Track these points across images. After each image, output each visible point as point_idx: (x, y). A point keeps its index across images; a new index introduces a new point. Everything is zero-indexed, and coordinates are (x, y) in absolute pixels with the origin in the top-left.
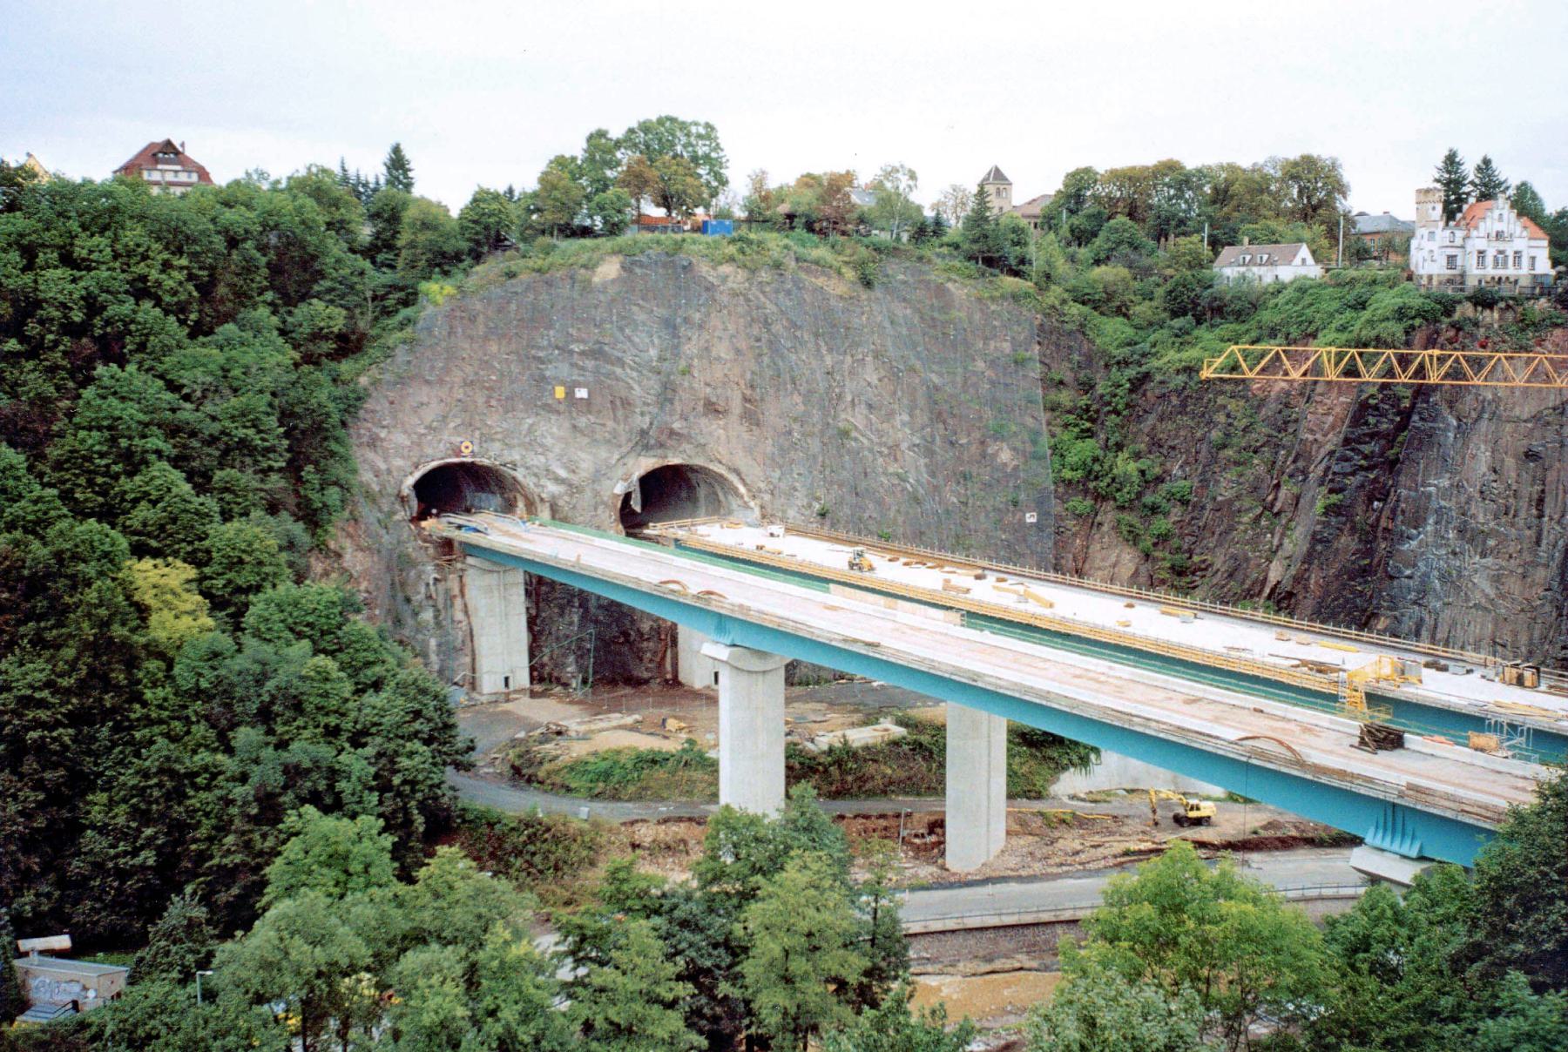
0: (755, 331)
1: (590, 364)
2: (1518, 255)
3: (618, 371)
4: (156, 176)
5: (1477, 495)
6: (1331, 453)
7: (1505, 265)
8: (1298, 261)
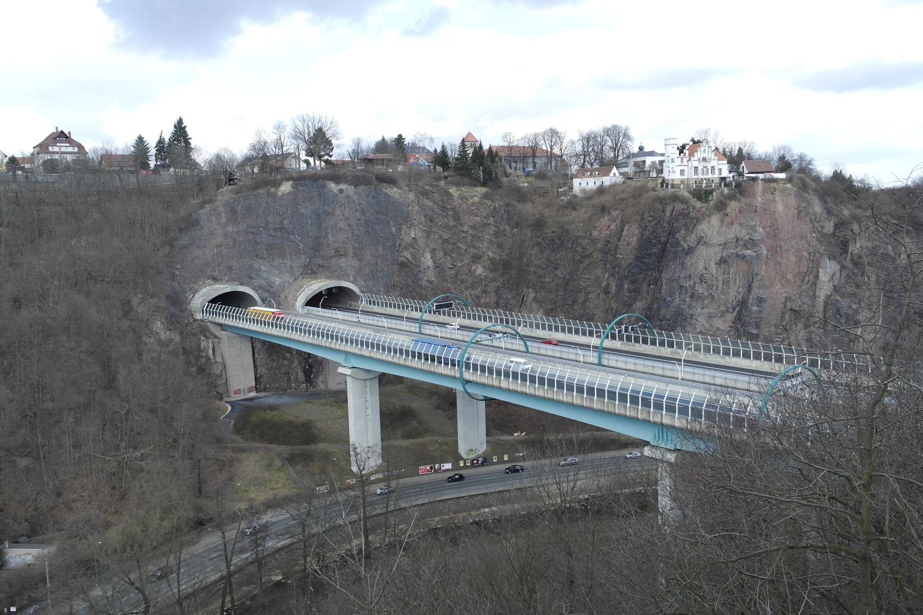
1: (279, 234)
2: (713, 168)
3: (292, 237)
4: (56, 149)
5: (698, 281)
6: (631, 264)
7: (707, 174)
8: (612, 174)
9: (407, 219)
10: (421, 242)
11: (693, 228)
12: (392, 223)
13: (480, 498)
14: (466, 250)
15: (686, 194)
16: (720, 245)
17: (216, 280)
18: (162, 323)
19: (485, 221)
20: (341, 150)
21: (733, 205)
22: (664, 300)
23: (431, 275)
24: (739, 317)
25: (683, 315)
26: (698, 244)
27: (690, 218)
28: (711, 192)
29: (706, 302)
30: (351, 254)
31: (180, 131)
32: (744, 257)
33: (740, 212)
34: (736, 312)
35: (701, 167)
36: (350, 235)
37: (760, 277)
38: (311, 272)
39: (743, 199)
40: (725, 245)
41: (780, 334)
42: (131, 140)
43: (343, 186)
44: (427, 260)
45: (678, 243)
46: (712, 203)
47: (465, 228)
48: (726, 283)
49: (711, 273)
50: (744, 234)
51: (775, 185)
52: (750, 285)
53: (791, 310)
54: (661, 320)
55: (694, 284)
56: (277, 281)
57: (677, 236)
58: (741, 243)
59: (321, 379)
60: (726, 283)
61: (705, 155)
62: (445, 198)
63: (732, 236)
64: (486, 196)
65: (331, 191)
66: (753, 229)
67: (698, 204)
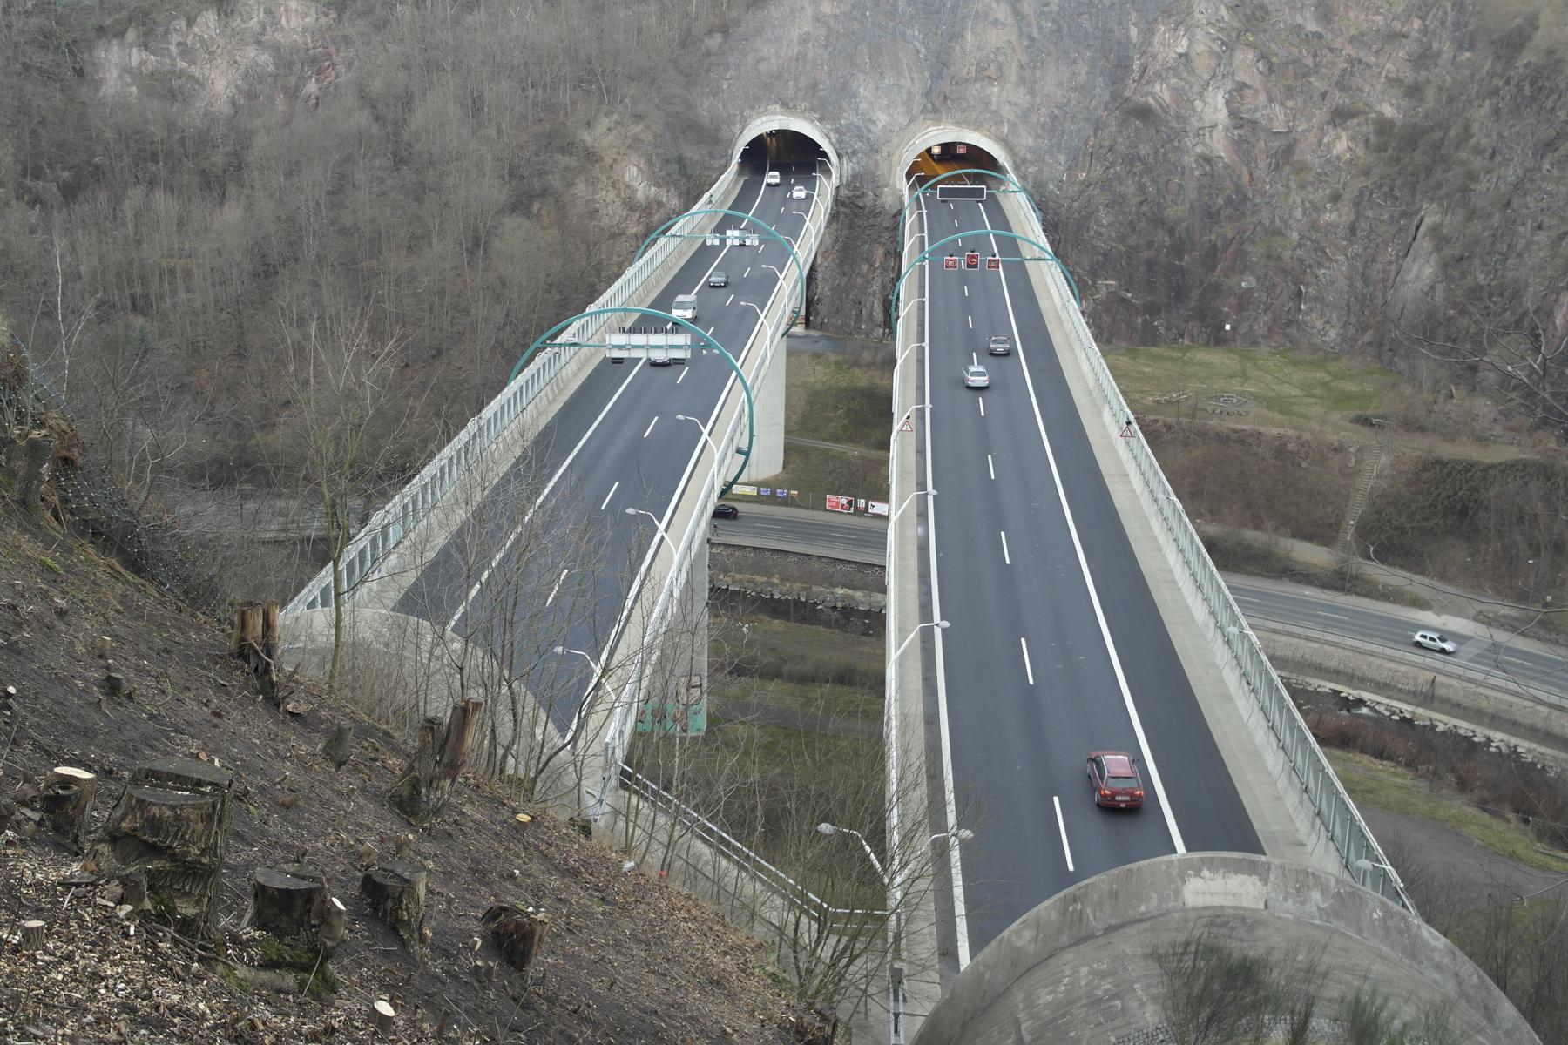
3: (909, 32)
10: (1203, 66)
12: (1134, 16)
13: (849, 568)
14: (1324, 95)
17: (787, 106)
18: (640, 169)
19: (1397, 25)
23: (1218, 144)
36: (1013, 38)
38: (937, 105)
44: (1214, 108)
56: (882, 118)
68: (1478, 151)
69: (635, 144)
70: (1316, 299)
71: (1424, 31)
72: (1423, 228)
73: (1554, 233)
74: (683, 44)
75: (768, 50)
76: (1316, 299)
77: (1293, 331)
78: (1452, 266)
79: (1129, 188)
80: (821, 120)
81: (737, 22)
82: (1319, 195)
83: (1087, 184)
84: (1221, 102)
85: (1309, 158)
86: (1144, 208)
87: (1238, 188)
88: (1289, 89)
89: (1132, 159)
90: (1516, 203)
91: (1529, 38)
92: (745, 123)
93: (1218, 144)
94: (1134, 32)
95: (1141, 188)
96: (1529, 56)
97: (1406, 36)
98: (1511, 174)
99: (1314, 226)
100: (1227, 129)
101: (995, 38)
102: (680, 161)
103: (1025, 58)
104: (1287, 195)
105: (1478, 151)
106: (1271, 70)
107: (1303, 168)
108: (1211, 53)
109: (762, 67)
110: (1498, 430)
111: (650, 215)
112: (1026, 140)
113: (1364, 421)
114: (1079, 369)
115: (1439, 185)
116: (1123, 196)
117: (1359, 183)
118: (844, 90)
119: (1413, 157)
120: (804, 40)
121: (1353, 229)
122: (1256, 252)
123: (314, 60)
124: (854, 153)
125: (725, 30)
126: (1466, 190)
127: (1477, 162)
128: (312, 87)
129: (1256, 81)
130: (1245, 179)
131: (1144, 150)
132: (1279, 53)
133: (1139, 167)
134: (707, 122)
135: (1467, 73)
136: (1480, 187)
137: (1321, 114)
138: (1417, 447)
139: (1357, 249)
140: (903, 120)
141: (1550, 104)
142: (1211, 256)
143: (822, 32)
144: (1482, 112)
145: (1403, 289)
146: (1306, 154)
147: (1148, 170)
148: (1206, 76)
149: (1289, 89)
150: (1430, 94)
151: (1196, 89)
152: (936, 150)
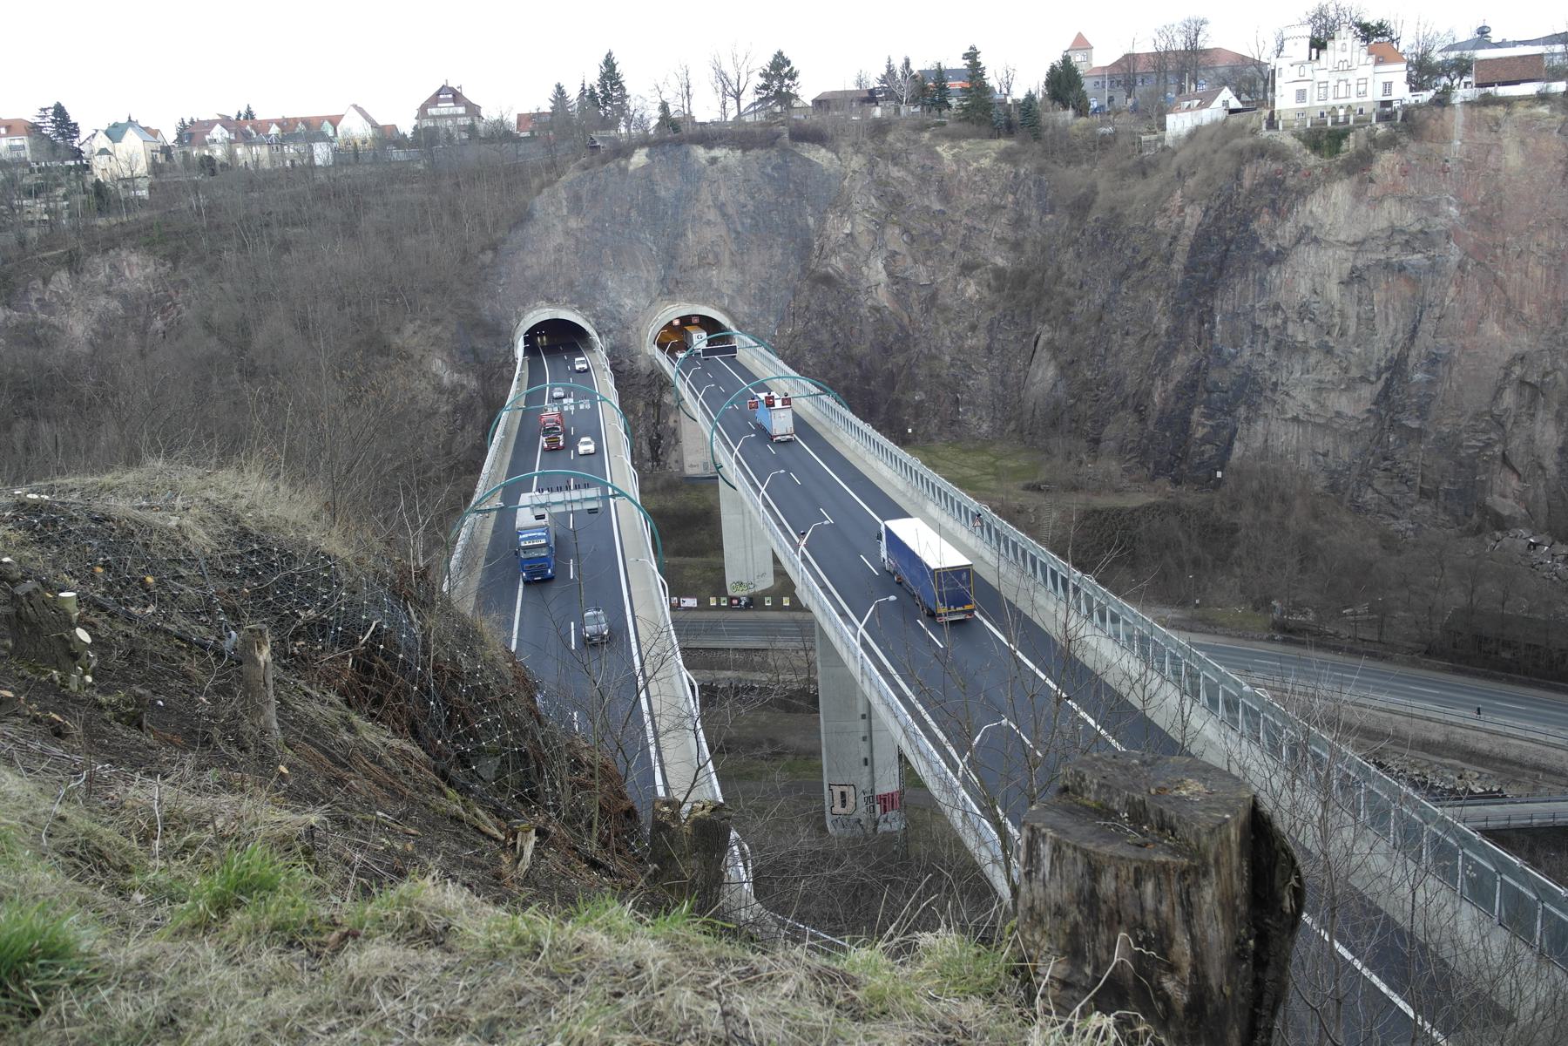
0: (742, 198)
5: (1295, 317)
8: (1217, 103)
9: (840, 203)
10: (864, 241)
11: (1290, 210)
12: (809, 209)
14: (953, 255)
15: (1289, 141)
16: (1354, 244)
17: (551, 301)
19: (997, 200)
20: (807, 91)
21: (1386, 161)
22: (1219, 352)
23: (883, 297)
24: (1384, 396)
25: (1254, 381)
26: (1298, 242)
27: (1286, 190)
28: (1343, 135)
29: (1312, 360)
30: (727, 263)
31: (610, 73)
32: (1402, 269)
33: (1404, 173)
34: (1380, 385)
35: (1333, 82)
36: (723, 232)
37: (1437, 311)
38: (670, 289)
39: (1413, 147)
40: (1359, 245)
41: (1484, 431)
42: (550, 91)
43: (718, 152)
44: (877, 271)
45: (1255, 240)
46: (1342, 157)
47: (957, 216)
48: (1368, 322)
49: (1328, 302)
50: (1409, 219)
51: (1500, 111)
52: (1415, 327)
53: (1522, 382)
54: (1210, 392)
55: (1285, 322)
57: (1255, 226)
58: (1399, 239)
59: (674, 456)
60: (1368, 322)
61: (1347, 56)
62: (928, 163)
63: (1385, 224)
64: (1007, 156)
65: (696, 160)
66: (1433, 208)
67: (1313, 160)
68: (1071, 284)
69: (437, 342)
70: (969, 403)
71: (1017, 203)
72: (1041, 343)
73: (1138, 337)
74: (463, 261)
75: (531, 260)
76: (969, 403)
77: (956, 428)
78: (1067, 368)
79: (824, 336)
80: (580, 308)
81: (504, 241)
82: (961, 327)
83: (794, 337)
84: (880, 266)
85: (949, 301)
86: (838, 350)
87: (902, 328)
88: (928, 252)
89: (823, 315)
90: (1106, 318)
91: (1093, 201)
92: (520, 317)
93: (883, 297)
94: (811, 221)
95: (833, 335)
96: (1095, 214)
97: (1004, 207)
98: (1098, 298)
99: (960, 350)
100: (887, 286)
101: (710, 234)
102: (474, 351)
103: (734, 247)
104: (937, 330)
105: (1071, 284)
106: (913, 240)
107: (945, 309)
108: (869, 231)
109: (528, 273)
110: (1126, 482)
111: (456, 396)
112: (742, 308)
113: (1036, 488)
114: (881, 476)
115: (1048, 311)
116: (821, 342)
117: (987, 317)
118: (595, 284)
119: (1024, 293)
120: (559, 249)
121: (989, 349)
122: (921, 373)
123: (157, 302)
124: (610, 331)
125: (494, 248)
126: (1066, 313)
127: (1070, 292)
128: (158, 324)
129: (903, 249)
130: (906, 320)
131: (831, 307)
132: (917, 227)
133: (829, 320)
134: (489, 319)
135: (1052, 230)
136: (1077, 309)
137: (953, 269)
138: (1077, 502)
139: (995, 363)
140: (644, 302)
141: (1117, 246)
142: (891, 380)
143: (572, 242)
144: (1068, 256)
145: (1033, 389)
146: (946, 298)
147: (836, 321)
148: (867, 248)
149: (928, 252)
150: (1028, 247)
151: (862, 258)
152: (677, 323)
